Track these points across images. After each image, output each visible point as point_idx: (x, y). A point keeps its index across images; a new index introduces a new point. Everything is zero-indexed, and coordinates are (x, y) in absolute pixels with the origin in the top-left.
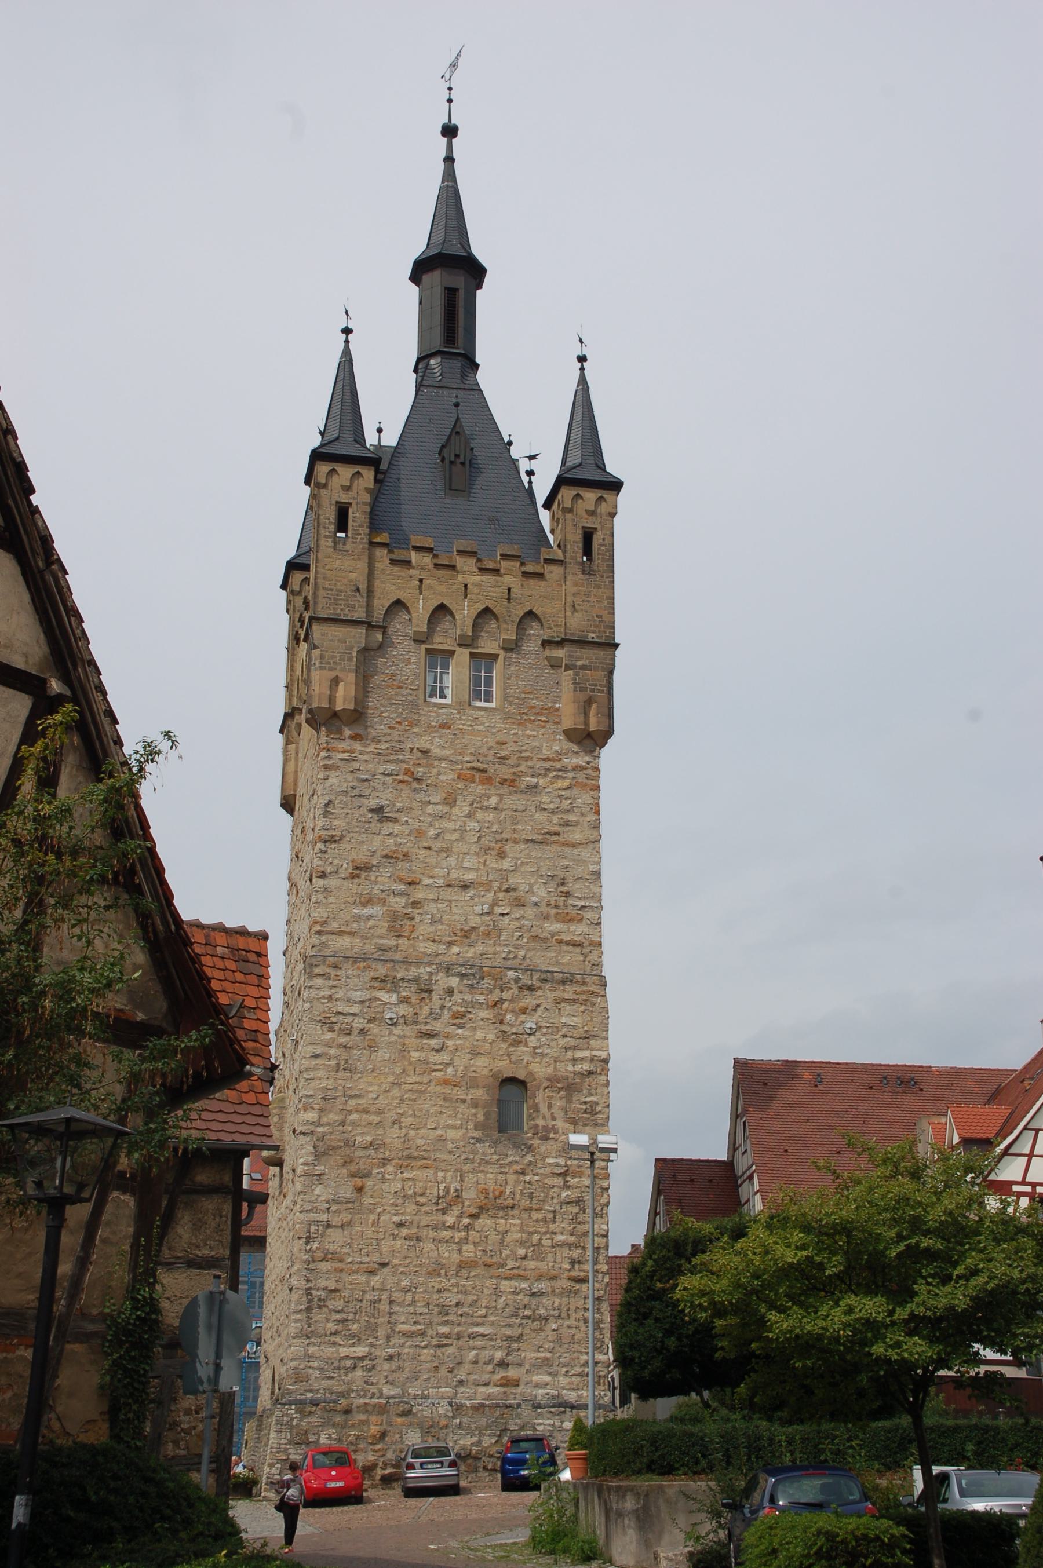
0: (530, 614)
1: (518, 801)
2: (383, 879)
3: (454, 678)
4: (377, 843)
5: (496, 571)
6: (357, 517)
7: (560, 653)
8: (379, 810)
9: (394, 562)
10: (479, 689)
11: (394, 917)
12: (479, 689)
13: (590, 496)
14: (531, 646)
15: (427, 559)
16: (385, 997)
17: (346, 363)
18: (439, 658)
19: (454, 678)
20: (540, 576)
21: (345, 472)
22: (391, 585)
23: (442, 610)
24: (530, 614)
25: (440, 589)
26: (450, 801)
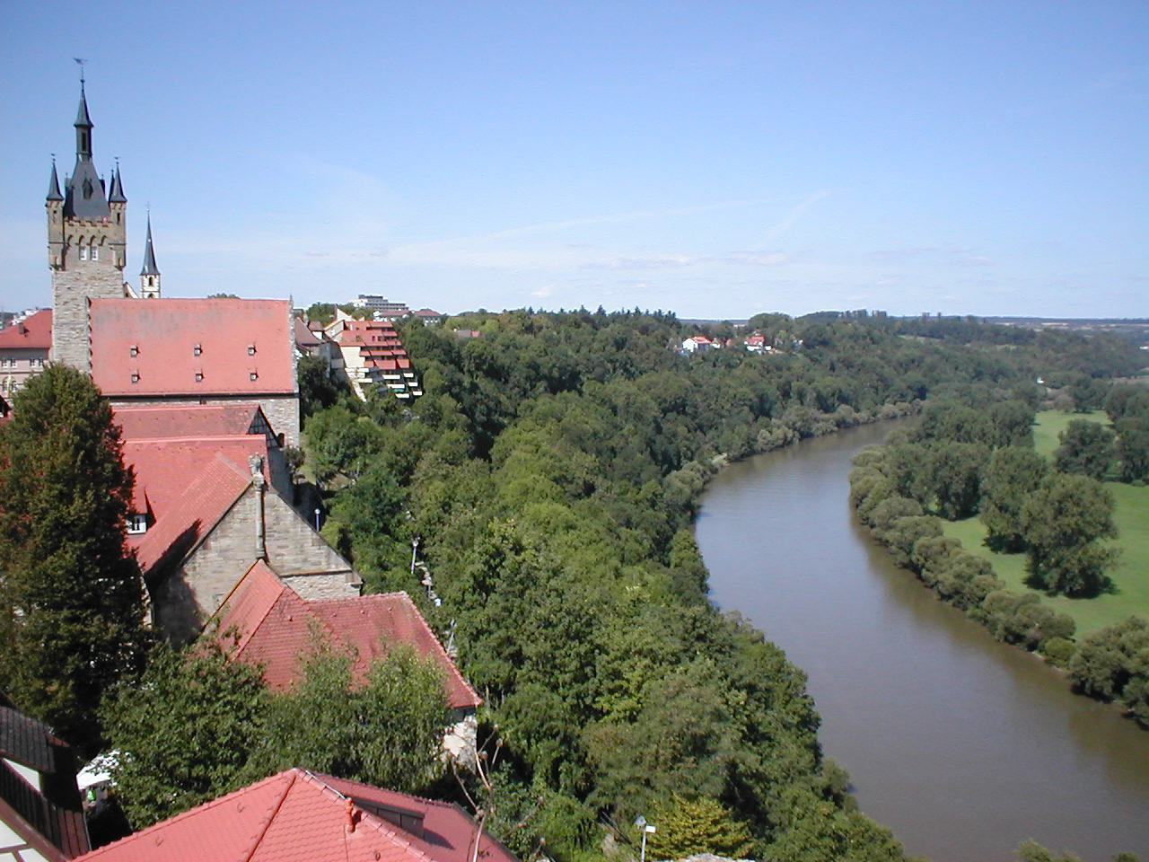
0: (105, 237)
1: (102, 283)
2: (71, 305)
3: (85, 253)
4: (68, 296)
5: (95, 226)
6: (60, 213)
7: (112, 246)
8: (69, 288)
9: (70, 225)
10: (91, 255)
11: (75, 313)
12: (91, 255)
13: (119, 205)
14: (105, 244)
15: (78, 224)
16: (73, 332)
17: (55, 170)
18: (82, 248)
19: (85, 253)
20: (107, 226)
21: (55, 203)
22: (69, 230)
23: (82, 237)
24: (105, 237)
25: (82, 231)
26: (86, 285)
